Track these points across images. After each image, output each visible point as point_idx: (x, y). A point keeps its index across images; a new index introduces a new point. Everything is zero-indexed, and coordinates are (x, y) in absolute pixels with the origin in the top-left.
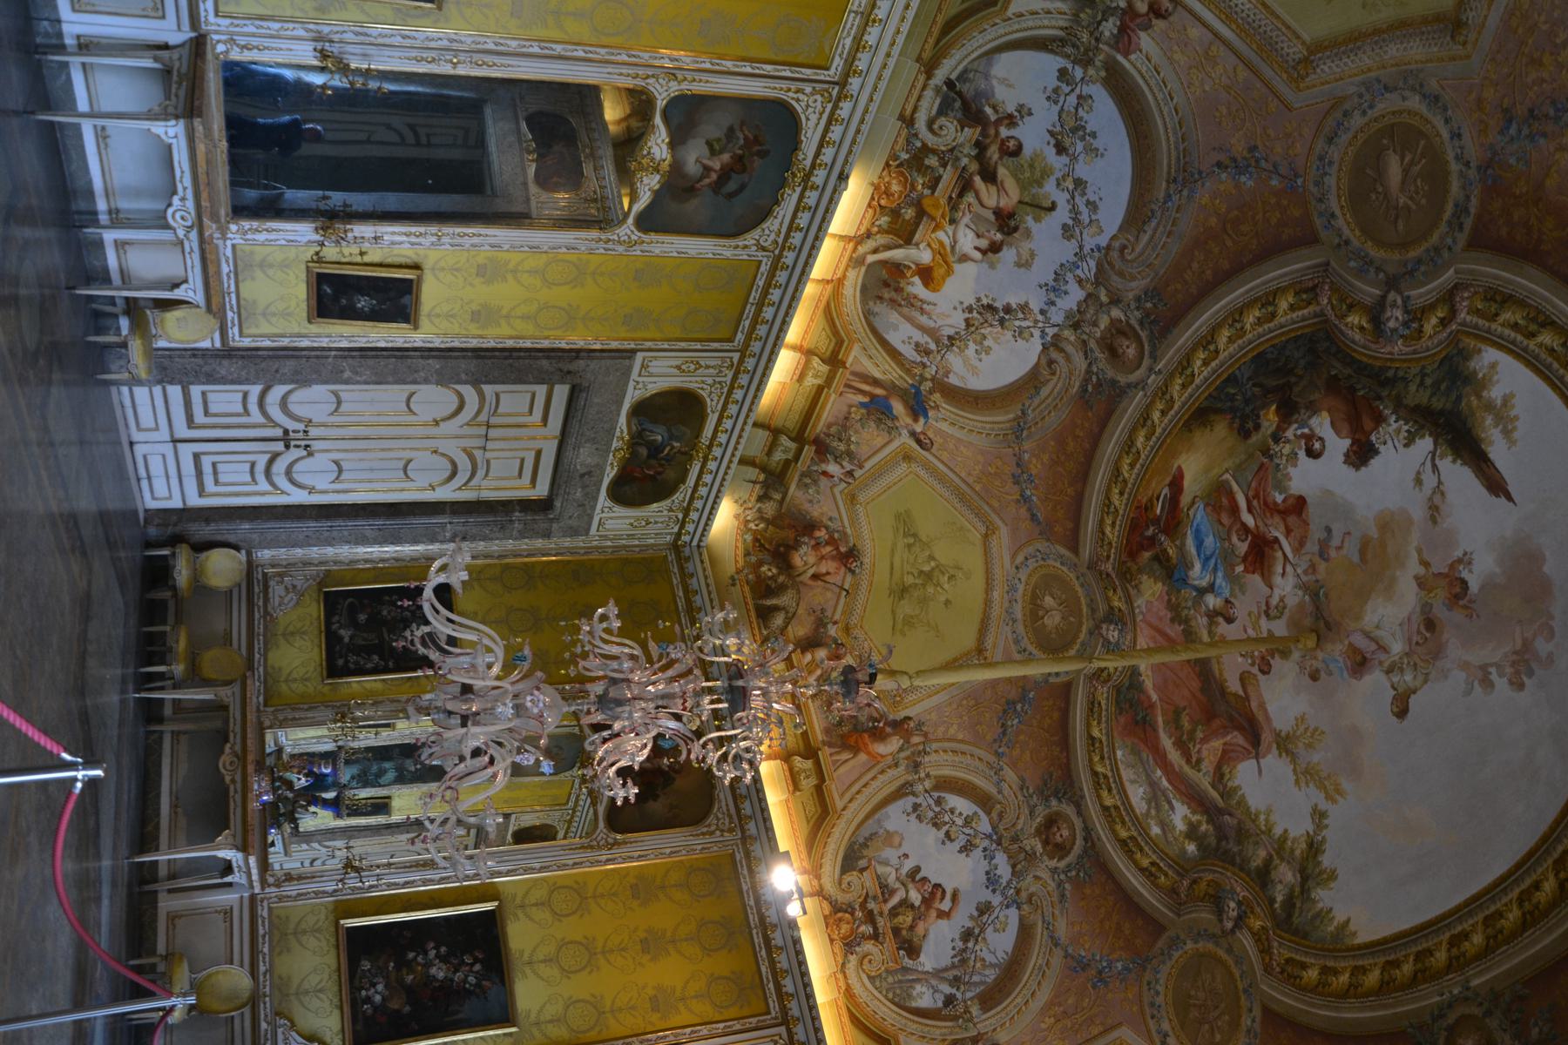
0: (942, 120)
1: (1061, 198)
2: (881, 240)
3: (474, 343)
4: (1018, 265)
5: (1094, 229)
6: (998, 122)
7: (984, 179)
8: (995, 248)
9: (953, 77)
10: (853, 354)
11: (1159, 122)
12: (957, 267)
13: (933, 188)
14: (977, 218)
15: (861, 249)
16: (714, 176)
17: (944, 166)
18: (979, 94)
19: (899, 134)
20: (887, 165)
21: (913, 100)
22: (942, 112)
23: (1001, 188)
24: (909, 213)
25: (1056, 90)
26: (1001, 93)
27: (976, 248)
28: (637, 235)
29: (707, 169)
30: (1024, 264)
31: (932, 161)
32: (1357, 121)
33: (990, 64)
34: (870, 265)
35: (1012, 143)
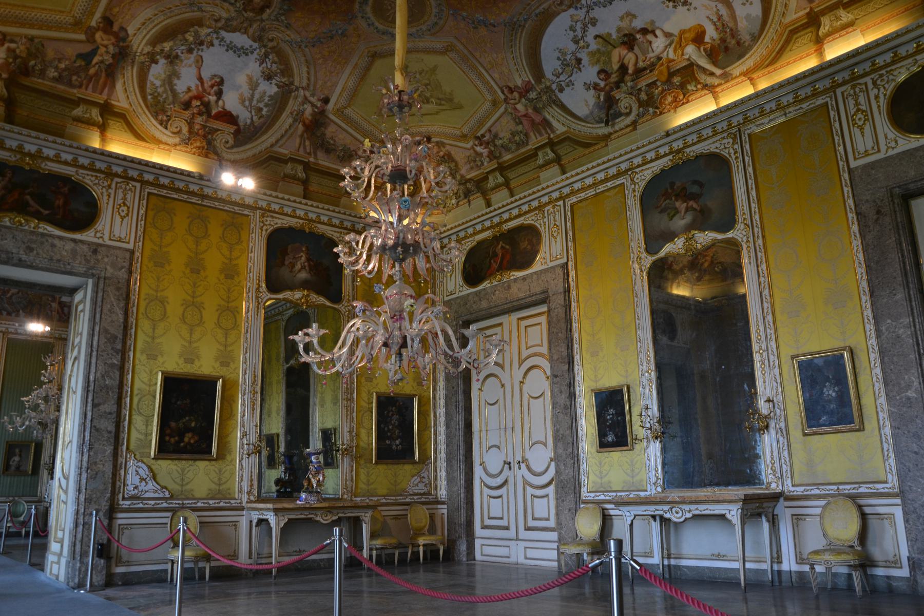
0: (623, 111)
1: (590, 38)
2: (703, 78)
3: (866, 298)
4: (634, 16)
5: (576, 18)
6: (602, 90)
7: (627, 69)
8: (644, 31)
9: (603, 125)
10: (795, 17)
11: (522, 50)
12: (676, 32)
13: (654, 83)
14: (645, 52)
15: (716, 81)
16: (691, 203)
17: (640, 89)
18: (600, 108)
19: (643, 122)
20: (661, 113)
21: (624, 131)
22: (620, 114)
23: (621, 59)
24: (676, 80)
25: (568, 86)
26: (592, 101)
27: (656, 36)
28: (740, 226)
29: (687, 210)
30: (631, 16)
31: (643, 96)
32: (424, 27)
33: (587, 116)
34: (723, 68)
35: (602, 76)
